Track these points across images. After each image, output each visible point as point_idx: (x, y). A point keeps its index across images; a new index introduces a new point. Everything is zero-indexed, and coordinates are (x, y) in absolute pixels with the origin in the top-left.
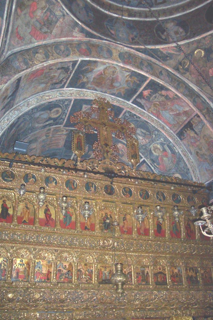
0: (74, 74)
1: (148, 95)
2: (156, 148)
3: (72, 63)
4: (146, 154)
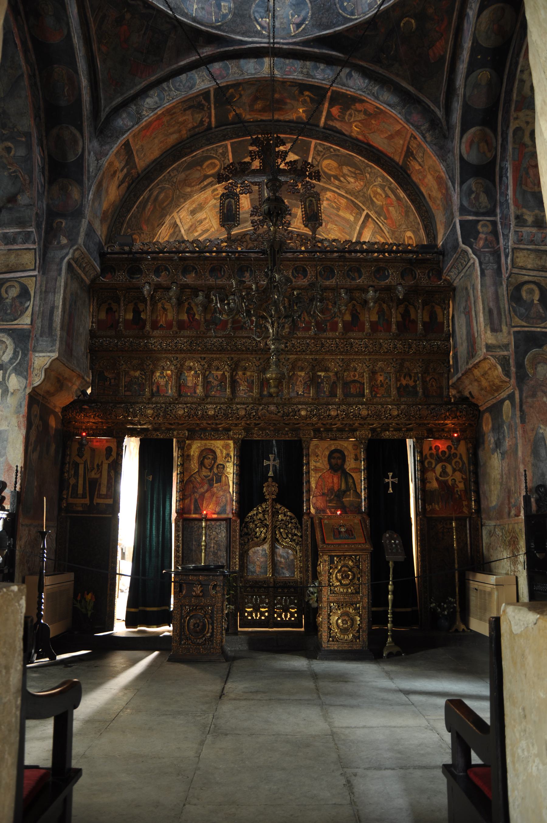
0: (215, 109)
2: (376, 193)
3: (201, 97)
4: (368, 204)
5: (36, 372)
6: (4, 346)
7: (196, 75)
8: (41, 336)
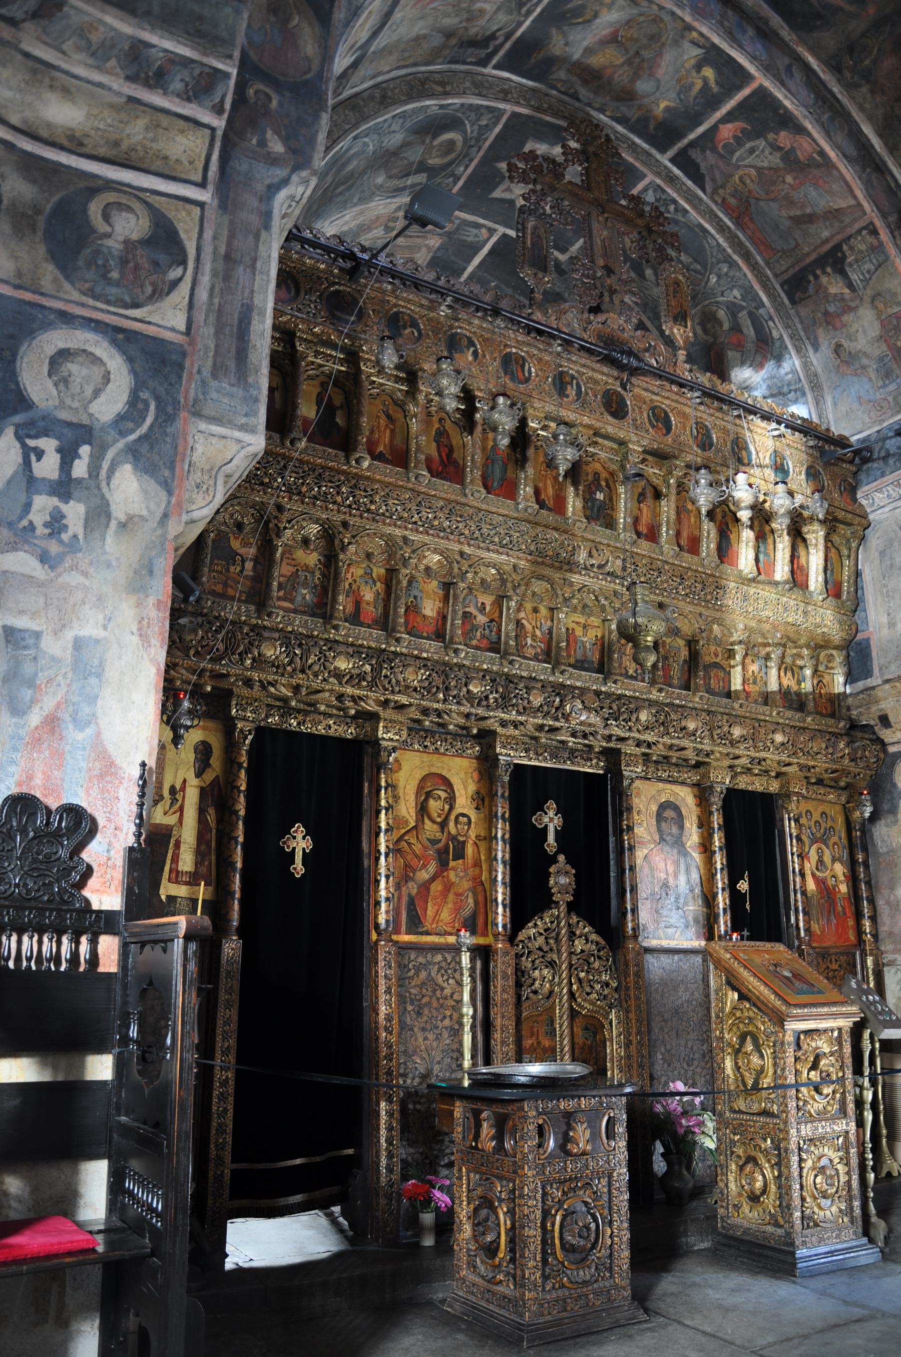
5: (197, 477)
6: (97, 372)
8: (214, 376)
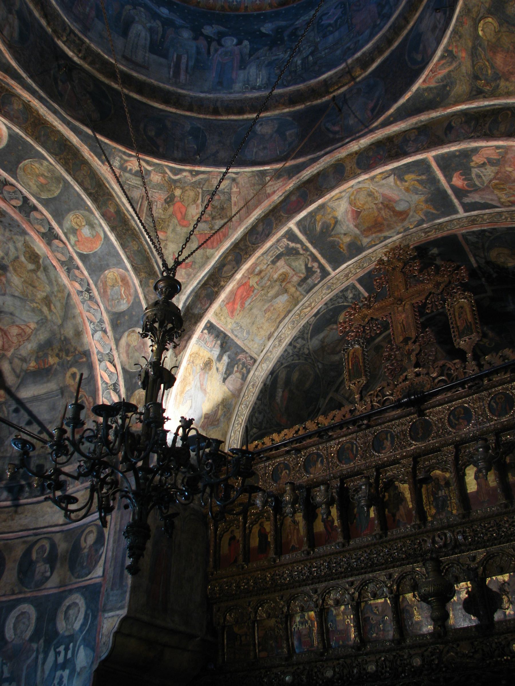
0: (315, 247)
1: (466, 182)
3: (285, 240)
6: (77, 609)
7: (273, 219)
8: (112, 589)
